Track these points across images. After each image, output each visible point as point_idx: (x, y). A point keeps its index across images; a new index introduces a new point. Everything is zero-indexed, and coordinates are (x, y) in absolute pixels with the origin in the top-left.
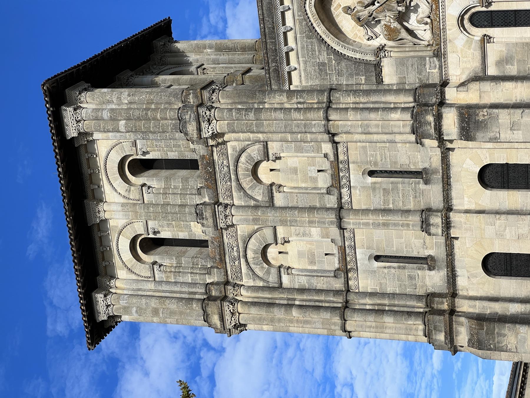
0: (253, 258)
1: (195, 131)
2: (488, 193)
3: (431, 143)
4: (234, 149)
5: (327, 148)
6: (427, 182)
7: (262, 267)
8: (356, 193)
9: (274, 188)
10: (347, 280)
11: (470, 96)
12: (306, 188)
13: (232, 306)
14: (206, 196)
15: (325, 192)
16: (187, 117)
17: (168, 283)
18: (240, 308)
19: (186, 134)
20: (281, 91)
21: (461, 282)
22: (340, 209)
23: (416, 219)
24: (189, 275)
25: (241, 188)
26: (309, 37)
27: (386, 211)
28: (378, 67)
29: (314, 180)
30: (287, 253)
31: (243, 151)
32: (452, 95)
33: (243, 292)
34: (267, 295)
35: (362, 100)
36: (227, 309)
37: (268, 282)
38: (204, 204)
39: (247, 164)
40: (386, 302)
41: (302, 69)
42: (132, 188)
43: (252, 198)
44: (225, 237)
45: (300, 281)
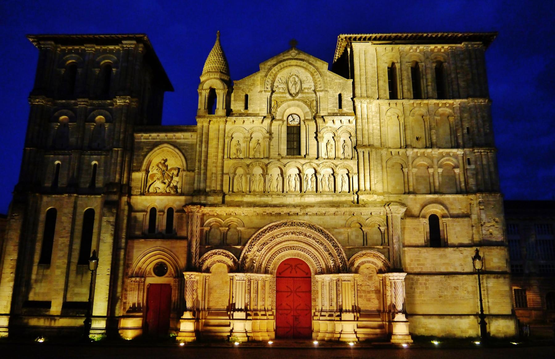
21: (45, 199)
32: (125, 199)
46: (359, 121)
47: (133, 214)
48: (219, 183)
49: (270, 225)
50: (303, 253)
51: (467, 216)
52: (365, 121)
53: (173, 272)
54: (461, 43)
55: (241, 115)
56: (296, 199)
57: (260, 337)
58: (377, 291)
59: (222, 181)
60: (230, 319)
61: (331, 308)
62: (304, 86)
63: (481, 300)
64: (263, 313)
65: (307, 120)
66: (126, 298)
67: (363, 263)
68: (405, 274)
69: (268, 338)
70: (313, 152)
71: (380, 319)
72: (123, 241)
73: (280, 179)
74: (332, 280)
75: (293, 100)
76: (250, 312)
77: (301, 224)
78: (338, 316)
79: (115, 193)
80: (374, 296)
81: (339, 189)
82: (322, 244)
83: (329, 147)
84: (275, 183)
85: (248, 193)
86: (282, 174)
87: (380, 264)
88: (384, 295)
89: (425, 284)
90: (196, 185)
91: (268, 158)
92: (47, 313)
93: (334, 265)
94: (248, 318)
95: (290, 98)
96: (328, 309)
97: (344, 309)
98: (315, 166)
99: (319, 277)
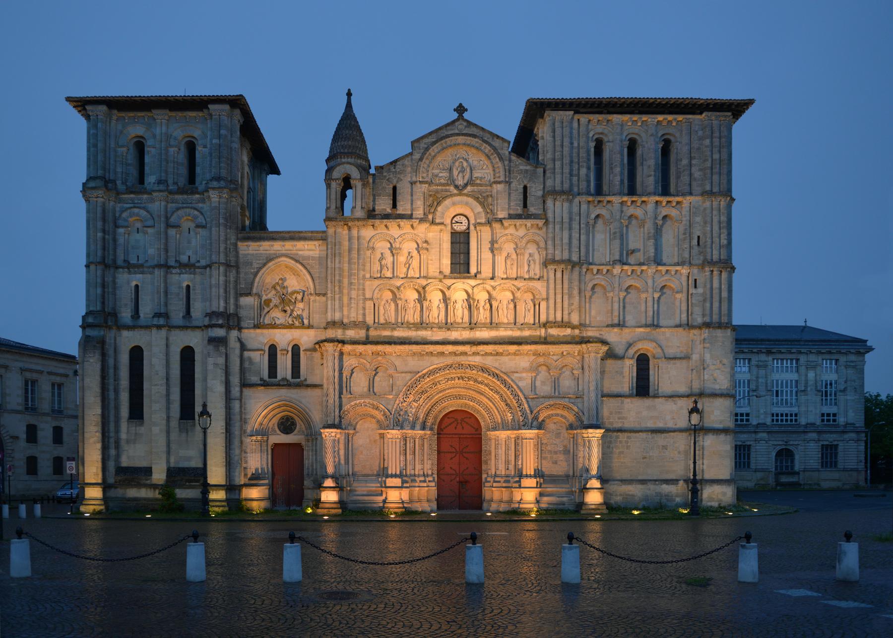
2: (179, 350)
3: (206, 321)
5: (203, 263)
6: (183, 317)
8: (176, 277)
10: (123, 268)
11: (234, 344)
19: (211, 180)
20: (238, 239)
21: (125, 333)
22: (167, 267)
23: (162, 311)
27: (166, 293)
28: (249, 294)
32: (234, 334)
33: (112, 203)
35: (232, 286)
38: (168, 186)
40: (110, 290)
46: (551, 226)
47: (246, 354)
48: (361, 312)
49: (431, 368)
50: (472, 403)
51: (687, 357)
52: (558, 227)
53: (304, 429)
54: (701, 113)
55: (387, 217)
56: (463, 333)
57: (418, 507)
58: (566, 451)
59: (364, 309)
60: (381, 487)
61: (508, 472)
62: (475, 175)
63: (695, 463)
64: (422, 479)
65: (480, 224)
66: (246, 462)
67: (549, 417)
68: (602, 431)
69: (428, 509)
70: (486, 271)
71: (568, 486)
72: (238, 389)
73: (442, 306)
74: (509, 438)
75: (460, 194)
76: (407, 480)
77: (470, 367)
78: (516, 482)
79: (221, 326)
80: (562, 457)
81: (520, 320)
82: (497, 392)
83: (509, 262)
84: (435, 312)
85: (400, 325)
86: (445, 300)
87: (571, 418)
88: (575, 457)
89: (627, 442)
90: (329, 314)
91: (426, 277)
92: (148, 482)
93: (513, 420)
94: (405, 485)
95: (455, 191)
96: (503, 473)
97: (524, 473)
98: (489, 288)
99: (492, 434)
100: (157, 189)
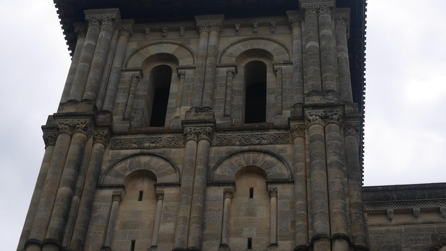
0: (139, 162)
1: (312, 103)
4: (283, 150)
7: (126, 170)
9: (230, 187)
12: (228, 222)
13: (83, 126)
14: (222, 122)
15: (223, 243)
16: (330, 97)
17: (119, 81)
18: (79, 136)
24: (124, 101)
25: (231, 155)
26: (434, 237)
29: (239, 234)
30: (140, 199)
31: (280, 159)
34: (91, 167)
36: (81, 121)
37: (106, 174)
39: (262, 162)
41: (391, 228)
42: (234, 59)
43: (219, 164)
44: (169, 136)
45: (102, 207)
100: (195, 118)
